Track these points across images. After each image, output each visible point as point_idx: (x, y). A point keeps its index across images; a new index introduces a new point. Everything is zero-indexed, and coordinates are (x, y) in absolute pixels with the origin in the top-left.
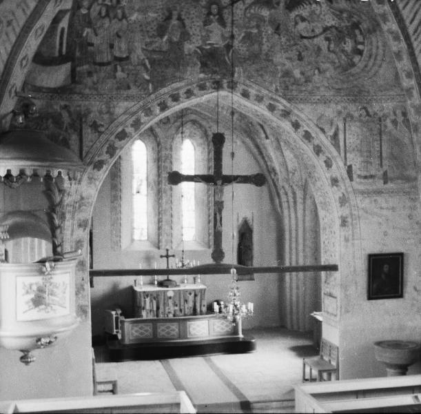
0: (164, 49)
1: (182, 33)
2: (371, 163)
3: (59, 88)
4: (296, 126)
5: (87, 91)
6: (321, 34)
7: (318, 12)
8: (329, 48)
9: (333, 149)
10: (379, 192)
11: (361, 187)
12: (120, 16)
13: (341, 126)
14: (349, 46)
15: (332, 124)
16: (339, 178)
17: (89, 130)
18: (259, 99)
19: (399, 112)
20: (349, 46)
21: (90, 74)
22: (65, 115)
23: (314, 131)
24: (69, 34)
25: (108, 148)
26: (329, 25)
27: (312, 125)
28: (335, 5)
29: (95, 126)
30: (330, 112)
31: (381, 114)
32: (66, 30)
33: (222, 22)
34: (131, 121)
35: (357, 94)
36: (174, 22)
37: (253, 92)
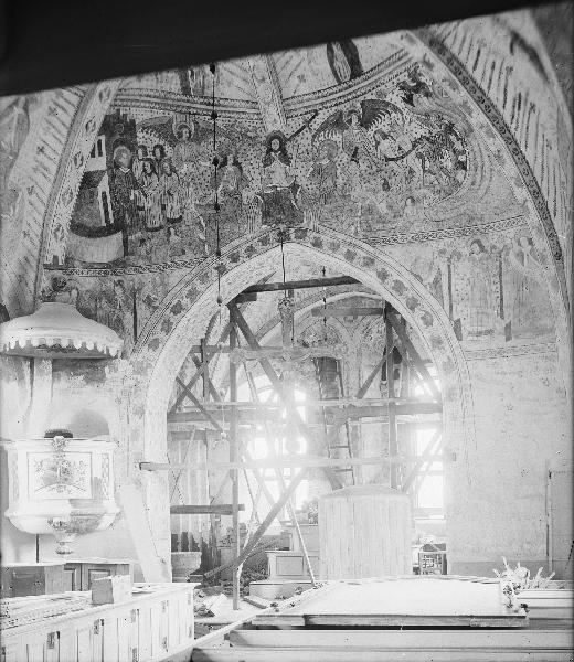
4: (383, 276)
5: (141, 262)
6: (410, 151)
7: (400, 122)
8: (423, 167)
9: (433, 301)
10: (501, 352)
11: (474, 348)
12: (168, 170)
13: (444, 270)
15: (431, 268)
16: (442, 336)
17: (143, 306)
18: (335, 247)
21: (143, 241)
22: (119, 291)
23: (407, 279)
24: (114, 198)
28: (418, 108)
32: (108, 194)
33: (286, 159)
34: (185, 293)
35: (469, 227)
36: (230, 168)
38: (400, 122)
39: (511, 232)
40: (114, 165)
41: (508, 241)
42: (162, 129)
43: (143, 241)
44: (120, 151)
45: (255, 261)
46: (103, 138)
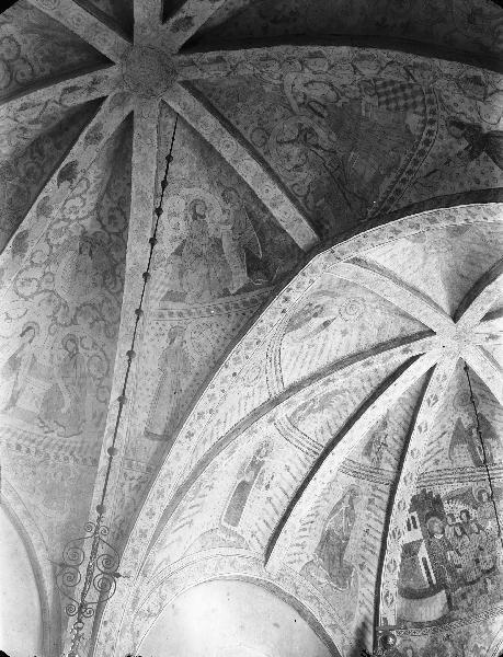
21: (464, 596)
32: (428, 560)
40: (430, 534)
42: (463, 497)
44: (434, 522)
46: (415, 514)
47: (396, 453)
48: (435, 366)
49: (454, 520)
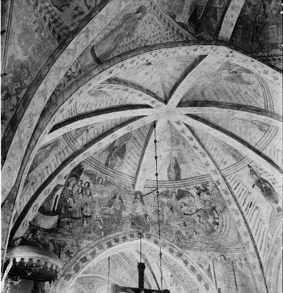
0: (111, 213)
1: (121, 206)
2: (231, 288)
3: (50, 229)
4: (186, 263)
7: (193, 201)
9: (208, 278)
14: (211, 220)
15: (206, 263)
17: (64, 255)
19: (243, 259)
20: (211, 220)
21: (68, 223)
22: (51, 245)
23: (196, 266)
24: (61, 198)
25: (75, 267)
26: (199, 208)
27: (195, 263)
29: (68, 253)
30: (204, 255)
31: (232, 259)
33: (142, 201)
35: (218, 248)
36: (117, 200)
37: (161, 241)
38: (193, 201)
39: (237, 254)
40: (67, 184)
41: (235, 258)
43: (68, 223)
44: (73, 180)
45: (127, 243)
47: (89, 138)
48: (144, 116)
49: (81, 184)
